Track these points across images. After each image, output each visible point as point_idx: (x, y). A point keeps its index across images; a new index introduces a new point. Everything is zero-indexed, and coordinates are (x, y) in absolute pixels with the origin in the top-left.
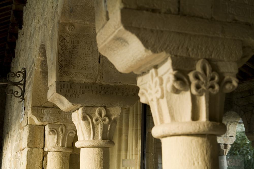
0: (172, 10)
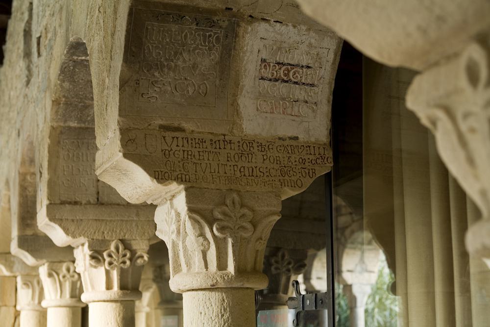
0: (92, 201)
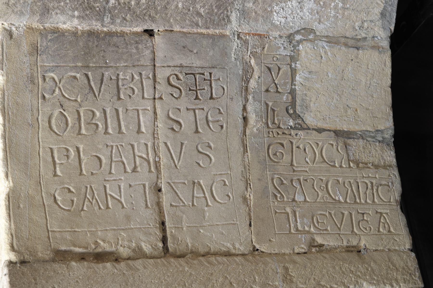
0: (146, 248)
